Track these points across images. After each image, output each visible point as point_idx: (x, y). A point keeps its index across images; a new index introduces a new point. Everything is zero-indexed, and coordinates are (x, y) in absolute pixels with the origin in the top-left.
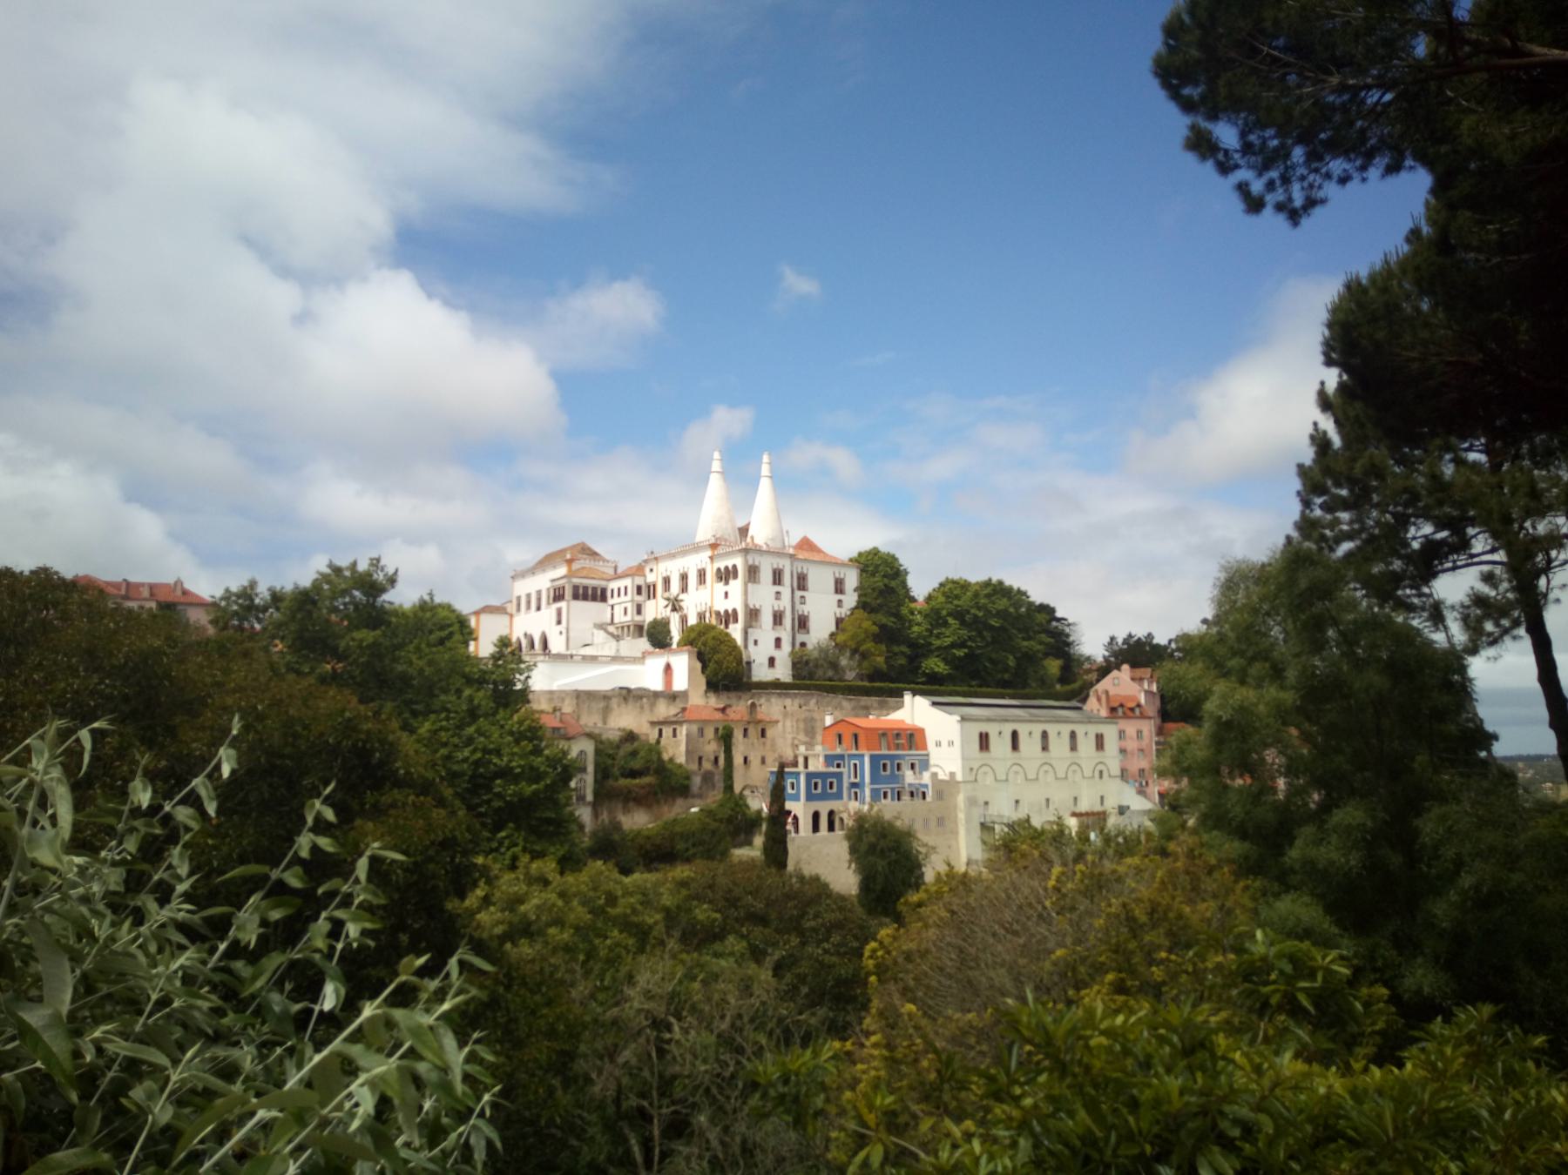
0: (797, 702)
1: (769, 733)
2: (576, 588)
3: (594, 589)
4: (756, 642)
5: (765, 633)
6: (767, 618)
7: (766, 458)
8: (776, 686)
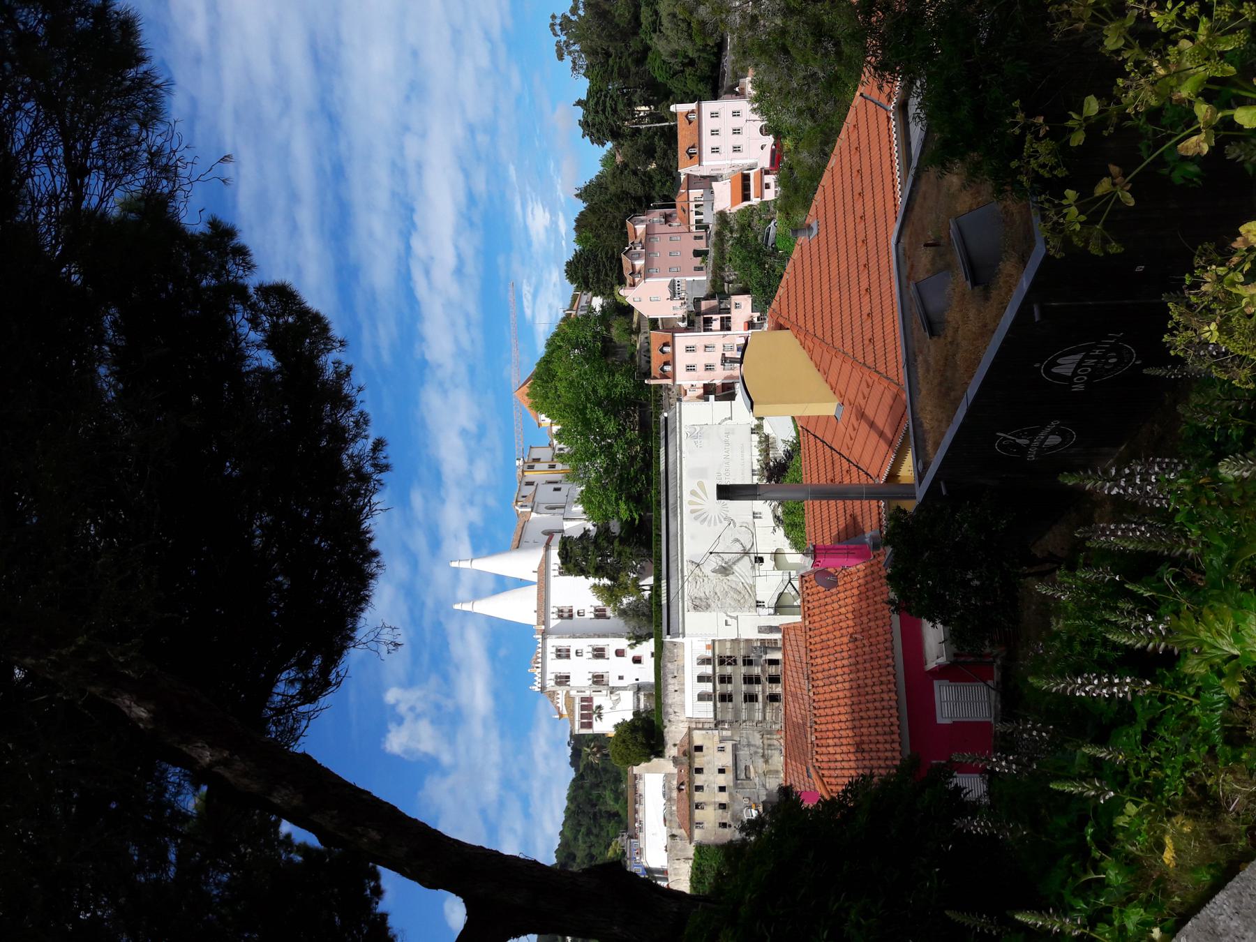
0: (671, 681)
1: (697, 742)
2: (583, 726)
3: (583, 708)
4: (621, 678)
5: (613, 667)
6: (599, 666)
7: (457, 607)
8: (658, 655)
